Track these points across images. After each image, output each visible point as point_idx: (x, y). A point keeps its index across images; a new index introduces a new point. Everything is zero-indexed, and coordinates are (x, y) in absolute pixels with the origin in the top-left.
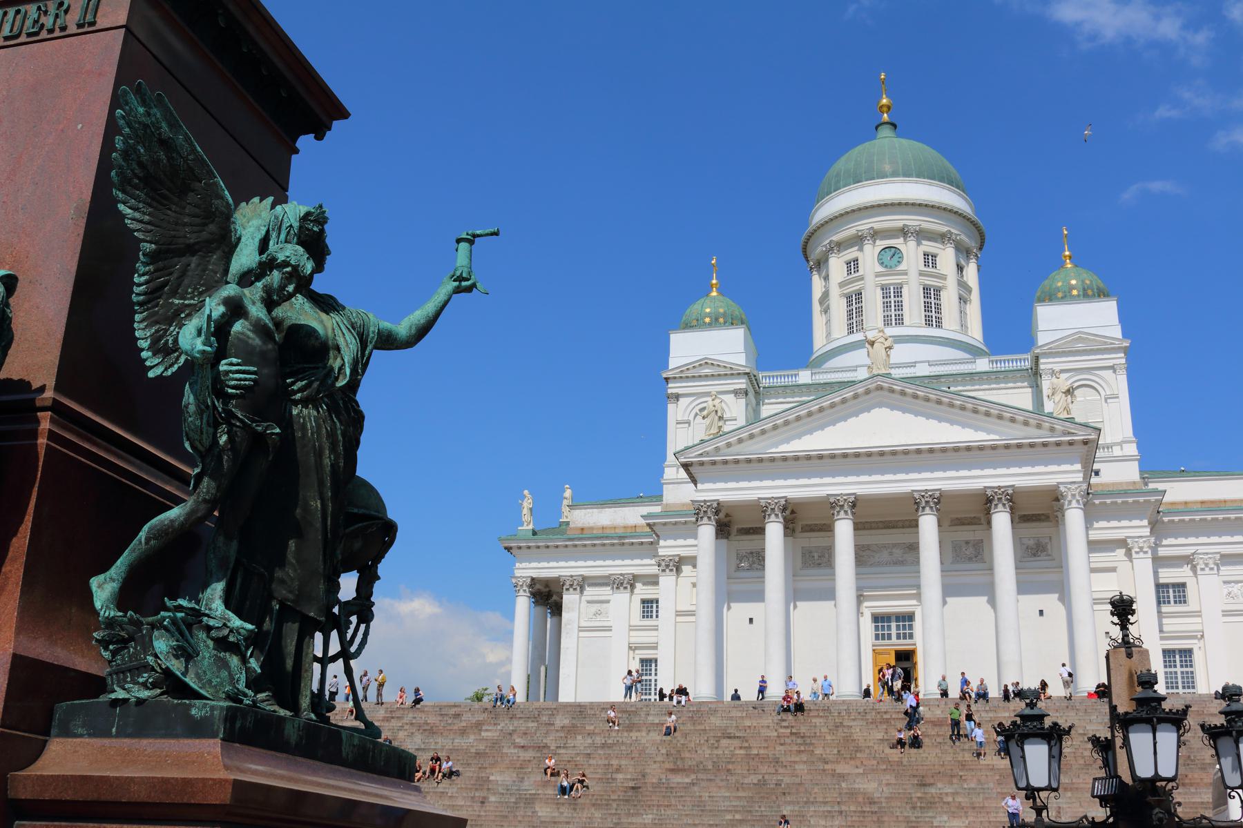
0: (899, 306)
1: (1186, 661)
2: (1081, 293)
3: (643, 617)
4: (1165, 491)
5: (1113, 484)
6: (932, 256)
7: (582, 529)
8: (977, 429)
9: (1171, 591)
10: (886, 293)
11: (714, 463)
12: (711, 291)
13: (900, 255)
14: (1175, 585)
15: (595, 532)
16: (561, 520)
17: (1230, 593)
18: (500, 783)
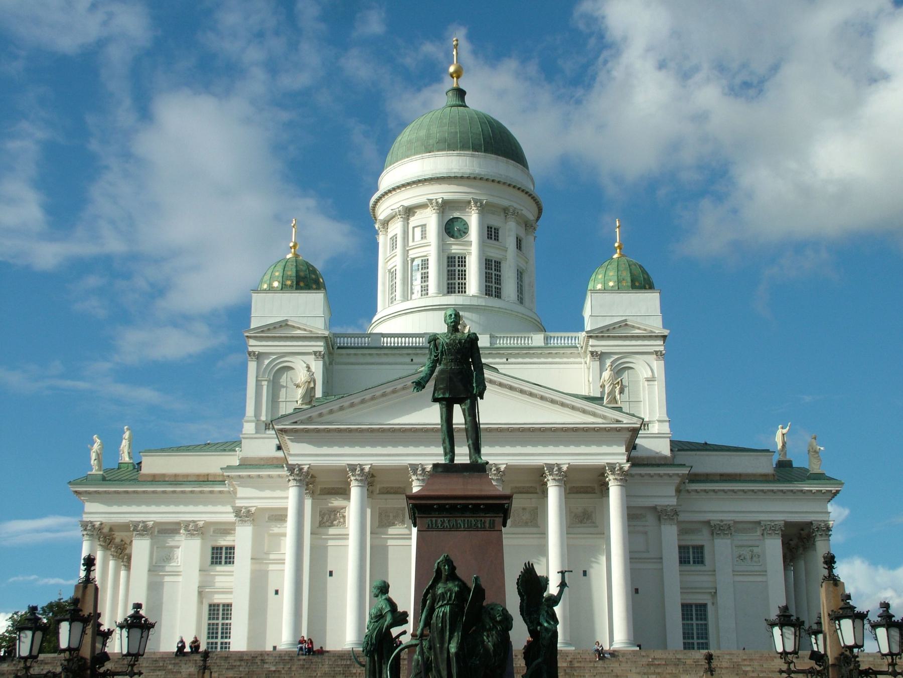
0: (463, 275)
1: (701, 615)
2: (629, 284)
3: (212, 563)
4: (692, 467)
5: (648, 458)
6: (495, 229)
7: (154, 476)
9: (691, 550)
10: (452, 262)
12: (291, 252)
13: (466, 226)
14: (694, 547)
15: (167, 479)
16: (120, 462)
17: (740, 556)
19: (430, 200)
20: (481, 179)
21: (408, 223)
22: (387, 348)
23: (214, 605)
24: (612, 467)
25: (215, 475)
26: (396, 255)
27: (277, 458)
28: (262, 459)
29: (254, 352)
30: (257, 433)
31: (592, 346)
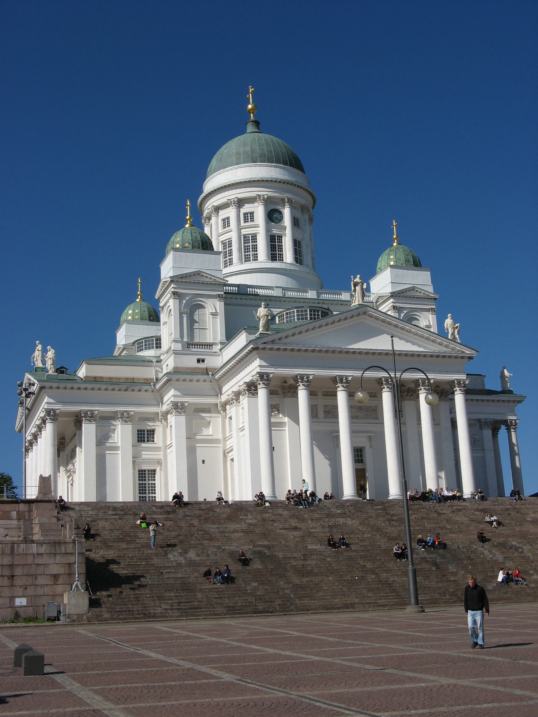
0: (281, 248)
7: (95, 378)
8: (413, 344)
11: (271, 349)
12: (187, 223)
13: (281, 216)
15: (104, 380)
18: (318, 550)
19: (259, 196)
20: (291, 184)
21: (240, 211)
22: (250, 295)
23: (142, 471)
24: (459, 382)
25: (138, 379)
26: (231, 231)
27: (199, 368)
28: (188, 368)
29: (177, 292)
30: (183, 350)
31: (393, 302)
